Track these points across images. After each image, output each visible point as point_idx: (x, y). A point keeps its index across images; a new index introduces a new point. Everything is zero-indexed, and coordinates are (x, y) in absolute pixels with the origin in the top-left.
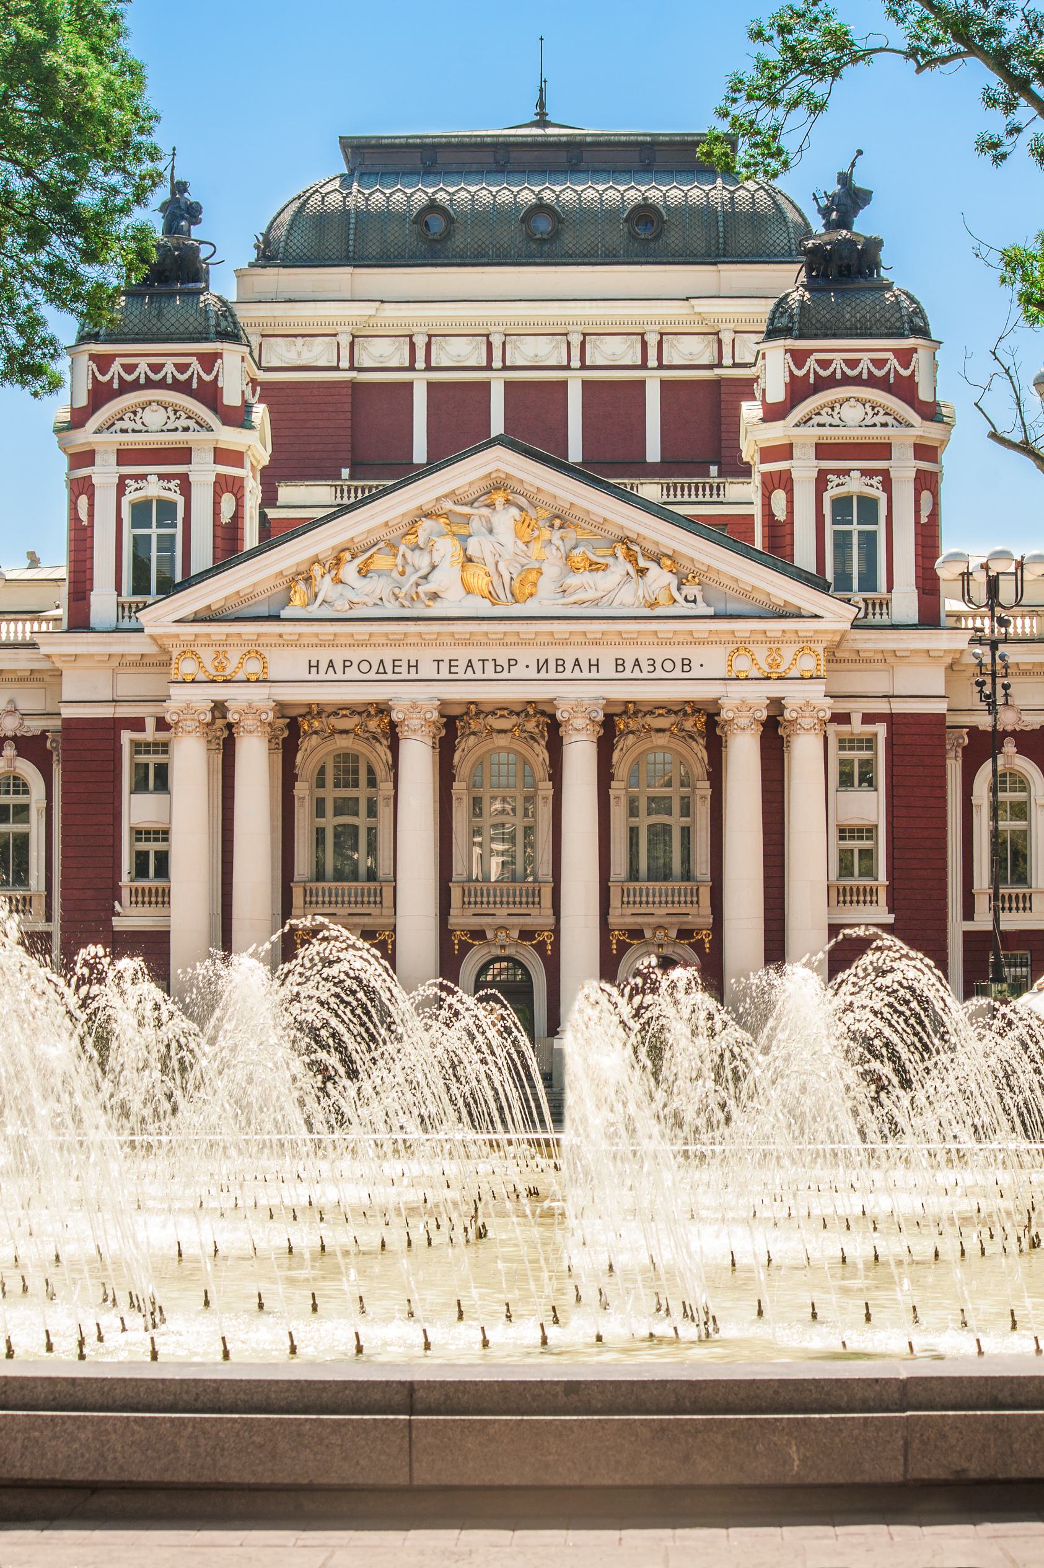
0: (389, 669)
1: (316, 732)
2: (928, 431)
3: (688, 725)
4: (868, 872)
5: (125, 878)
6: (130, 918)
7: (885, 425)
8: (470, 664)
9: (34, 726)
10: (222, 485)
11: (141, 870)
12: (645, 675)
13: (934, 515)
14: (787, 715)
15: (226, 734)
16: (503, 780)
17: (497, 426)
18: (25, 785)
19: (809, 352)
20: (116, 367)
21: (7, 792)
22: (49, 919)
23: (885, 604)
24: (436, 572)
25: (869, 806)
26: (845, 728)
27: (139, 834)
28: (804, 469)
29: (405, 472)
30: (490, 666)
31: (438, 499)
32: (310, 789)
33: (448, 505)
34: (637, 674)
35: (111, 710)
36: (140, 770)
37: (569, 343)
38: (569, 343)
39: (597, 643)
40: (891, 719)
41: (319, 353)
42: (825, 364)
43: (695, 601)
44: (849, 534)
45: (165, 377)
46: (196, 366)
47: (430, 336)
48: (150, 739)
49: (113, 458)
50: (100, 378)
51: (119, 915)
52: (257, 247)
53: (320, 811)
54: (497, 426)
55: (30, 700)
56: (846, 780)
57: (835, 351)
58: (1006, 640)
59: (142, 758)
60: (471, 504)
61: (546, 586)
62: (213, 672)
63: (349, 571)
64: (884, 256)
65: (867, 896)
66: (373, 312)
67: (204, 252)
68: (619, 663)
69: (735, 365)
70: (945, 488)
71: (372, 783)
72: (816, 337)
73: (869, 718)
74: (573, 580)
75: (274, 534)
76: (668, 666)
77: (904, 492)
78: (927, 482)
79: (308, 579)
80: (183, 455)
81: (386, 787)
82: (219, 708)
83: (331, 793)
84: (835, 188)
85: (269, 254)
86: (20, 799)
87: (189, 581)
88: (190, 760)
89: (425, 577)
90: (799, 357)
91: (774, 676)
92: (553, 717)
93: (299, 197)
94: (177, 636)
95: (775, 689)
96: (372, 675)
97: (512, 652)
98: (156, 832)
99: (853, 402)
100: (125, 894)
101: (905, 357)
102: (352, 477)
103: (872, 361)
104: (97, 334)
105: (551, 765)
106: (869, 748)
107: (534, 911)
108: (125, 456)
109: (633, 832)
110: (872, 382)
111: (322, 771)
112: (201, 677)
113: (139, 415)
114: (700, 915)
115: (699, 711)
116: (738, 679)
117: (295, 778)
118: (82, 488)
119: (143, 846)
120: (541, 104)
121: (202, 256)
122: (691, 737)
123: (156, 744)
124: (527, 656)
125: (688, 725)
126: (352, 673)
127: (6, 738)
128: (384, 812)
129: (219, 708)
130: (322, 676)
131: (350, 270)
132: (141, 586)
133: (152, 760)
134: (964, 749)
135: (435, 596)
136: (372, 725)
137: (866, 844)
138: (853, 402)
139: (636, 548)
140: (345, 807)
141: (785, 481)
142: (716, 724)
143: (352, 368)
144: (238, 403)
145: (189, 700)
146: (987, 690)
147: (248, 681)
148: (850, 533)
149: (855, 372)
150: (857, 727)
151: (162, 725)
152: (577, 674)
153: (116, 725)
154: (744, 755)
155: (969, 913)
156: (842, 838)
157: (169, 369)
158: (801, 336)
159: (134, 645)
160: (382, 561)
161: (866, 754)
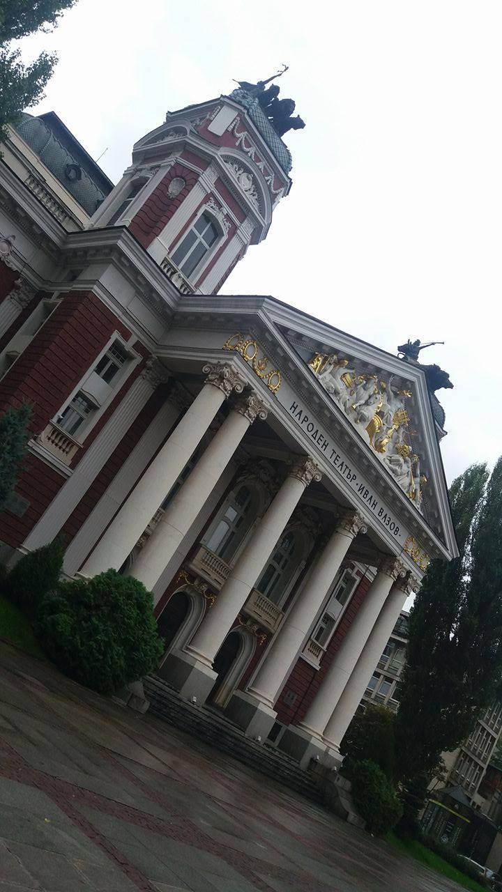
0: (317, 438)
12: (384, 524)
35: (120, 313)
73: (358, 573)
84: (413, 341)
94: (264, 329)
96: (310, 434)
113: (240, 172)
126: (304, 426)
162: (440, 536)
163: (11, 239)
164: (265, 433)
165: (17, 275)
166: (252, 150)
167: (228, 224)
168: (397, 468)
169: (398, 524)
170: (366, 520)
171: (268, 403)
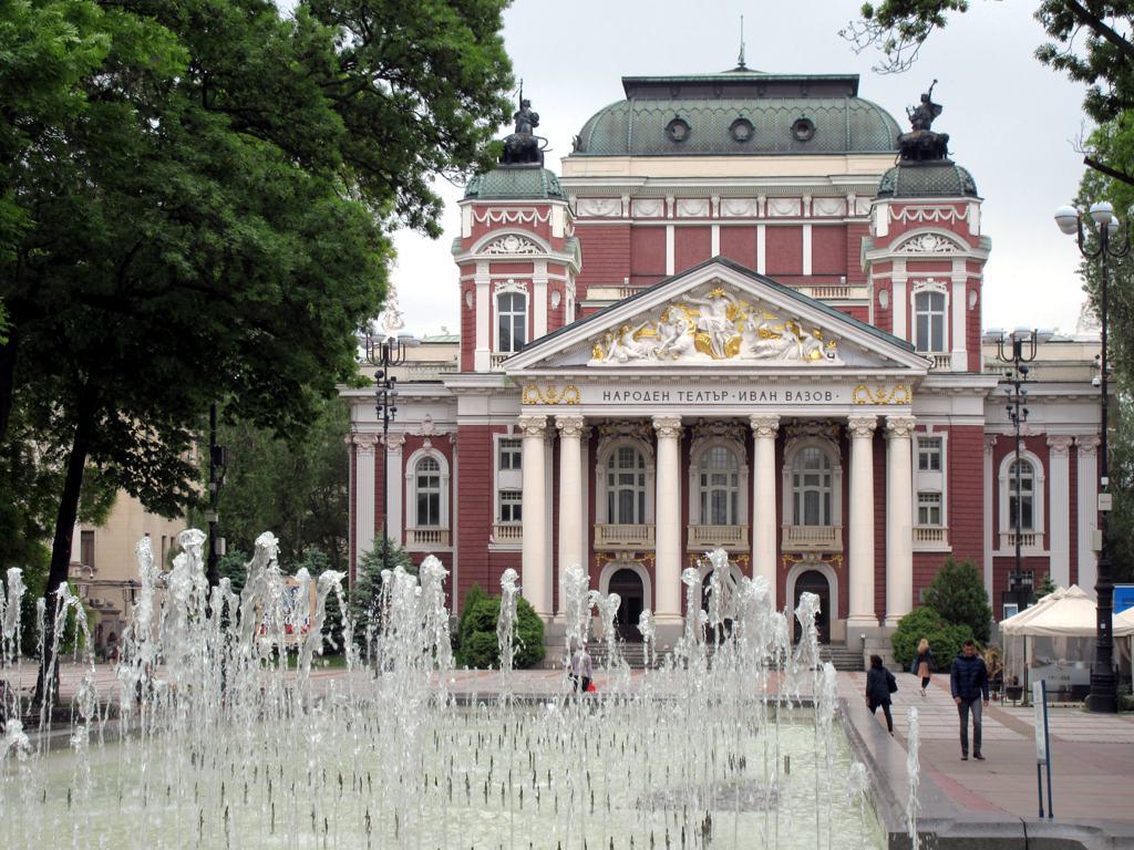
0: (652, 397)
1: (609, 435)
2: (977, 254)
3: (829, 432)
4: (936, 520)
5: (496, 522)
6: (499, 543)
7: (948, 250)
8: (700, 395)
9: (442, 430)
10: (555, 287)
11: (505, 516)
13: (978, 305)
14: (890, 425)
15: (555, 435)
16: (719, 464)
17: (715, 252)
18: (437, 465)
19: (903, 205)
20: (488, 214)
21: (426, 469)
22: (451, 544)
23: (947, 359)
24: (680, 338)
25: (937, 481)
26: (922, 434)
27: (504, 494)
28: (899, 274)
29: (662, 280)
30: (711, 396)
31: (681, 295)
32: (605, 468)
33: (686, 298)
34: (799, 401)
36: (505, 457)
37: (758, 203)
38: (758, 203)
39: (774, 382)
40: (951, 429)
41: (610, 209)
42: (912, 212)
43: (833, 357)
44: (926, 316)
45: (517, 220)
46: (536, 214)
47: (676, 199)
48: (510, 438)
49: (487, 269)
50: (479, 220)
51: (490, 542)
52: (574, 144)
53: (612, 482)
54: (715, 252)
55: (438, 414)
56: (923, 465)
57: (920, 207)
58: (1025, 382)
59: (506, 450)
60: (700, 297)
61: (745, 348)
62: (547, 400)
63: (629, 336)
64: (950, 146)
65: (934, 534)
66: (642, 184)
67: (541, 144)
68: (788, 395)
69: (856, 217)
70: (984, 290)
71: (642, 465)
72: (907, 196)
73: (937, 428)
74: (761, 343)
75: (583, 315)
76: (818, 396)
77: (960, 292)
78: (974, 286)
79: (604, 342)
80: (528, 266)
81: (649, 468)
82: (551, 420)
83: (617, 471)
84: (919, 103)
85: (580, 147)
86: (434, 473)
87: (534, 344)
88: (534, 451)
89: (673, 341)
90: (897, 208)
91: (881, 401)
92: (749, 426)
93: (599, 114)
94: (525, 377)
95: (882, 411)
96: (641, 401)
97: (723, 388)
98: (514, 493)
99: (929, 236)
100: (496, 530)
101: (962, 207)
102: (631, 282)
103: (941, 211)
104: (477, 193)
105: (748, 455)
106: (937, 446)
107: (737, 543)
108: (495, 266)
109: (796, 496)
110: (942, 223)
111: (612, 458)
112: (540, 402)
114: (837, 546)
115: (835, 423)
116: (859, 404)
117: (596, 462)
118: (468, 288)
119: (506, 502)
120: (741, 58)
121: (539, 146)
122: (831, 439)
123: (514, 441)
124: (734, 391)
125: (829, 432)
126: (630, 400)
127: (425, 436)
128: (649, 482)
129: (551, 420)
130: (612, 402)
131: (628, 158)
132: (504, 347)
133: (511, 450)
134: (994, 447)
135: (679, 352)
136: (642, 431)
137: (935, 504)
138: (929, 236)
139: (798, 324)
140: (627, 479)
141: (885, 286)
142: (846, 431)
143: (630, 218)
144: (562, 236)
145: (532, 415)
146: (1013, 411)
147: (568, 404)
148: (926, 316)
149: (930, 218)
150: (930, 433)
151: (517, 429)
152: (763, 401)
153: (489, 429)
154: (862, 451)
155: (996, 546)
156: (921, 500)
157: (520, 215)
158: (899, 196)
159: (498, 383)
160: (648, 332)
161: (935, 450)
162: (889, 363)
163: (428, 418)
164: (595, 433)
165: (447, 435)
166: (504, 214)
167: (522, 286)
168: (765, 353)
169: (823, 389)
170: (769, 416)
171: (576, 414)
